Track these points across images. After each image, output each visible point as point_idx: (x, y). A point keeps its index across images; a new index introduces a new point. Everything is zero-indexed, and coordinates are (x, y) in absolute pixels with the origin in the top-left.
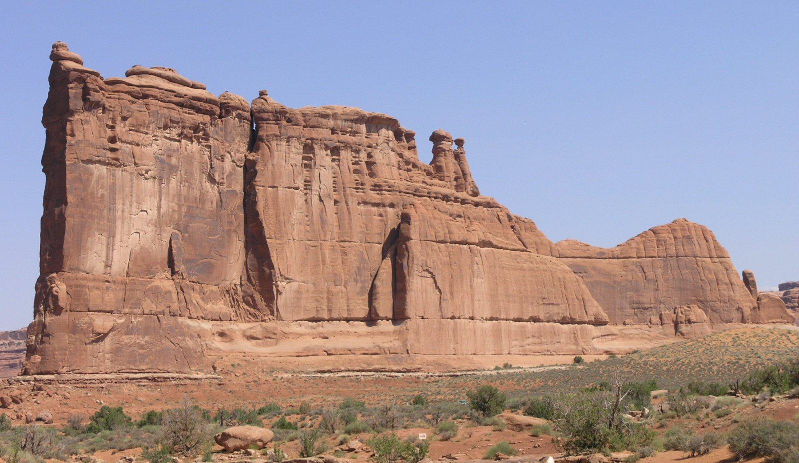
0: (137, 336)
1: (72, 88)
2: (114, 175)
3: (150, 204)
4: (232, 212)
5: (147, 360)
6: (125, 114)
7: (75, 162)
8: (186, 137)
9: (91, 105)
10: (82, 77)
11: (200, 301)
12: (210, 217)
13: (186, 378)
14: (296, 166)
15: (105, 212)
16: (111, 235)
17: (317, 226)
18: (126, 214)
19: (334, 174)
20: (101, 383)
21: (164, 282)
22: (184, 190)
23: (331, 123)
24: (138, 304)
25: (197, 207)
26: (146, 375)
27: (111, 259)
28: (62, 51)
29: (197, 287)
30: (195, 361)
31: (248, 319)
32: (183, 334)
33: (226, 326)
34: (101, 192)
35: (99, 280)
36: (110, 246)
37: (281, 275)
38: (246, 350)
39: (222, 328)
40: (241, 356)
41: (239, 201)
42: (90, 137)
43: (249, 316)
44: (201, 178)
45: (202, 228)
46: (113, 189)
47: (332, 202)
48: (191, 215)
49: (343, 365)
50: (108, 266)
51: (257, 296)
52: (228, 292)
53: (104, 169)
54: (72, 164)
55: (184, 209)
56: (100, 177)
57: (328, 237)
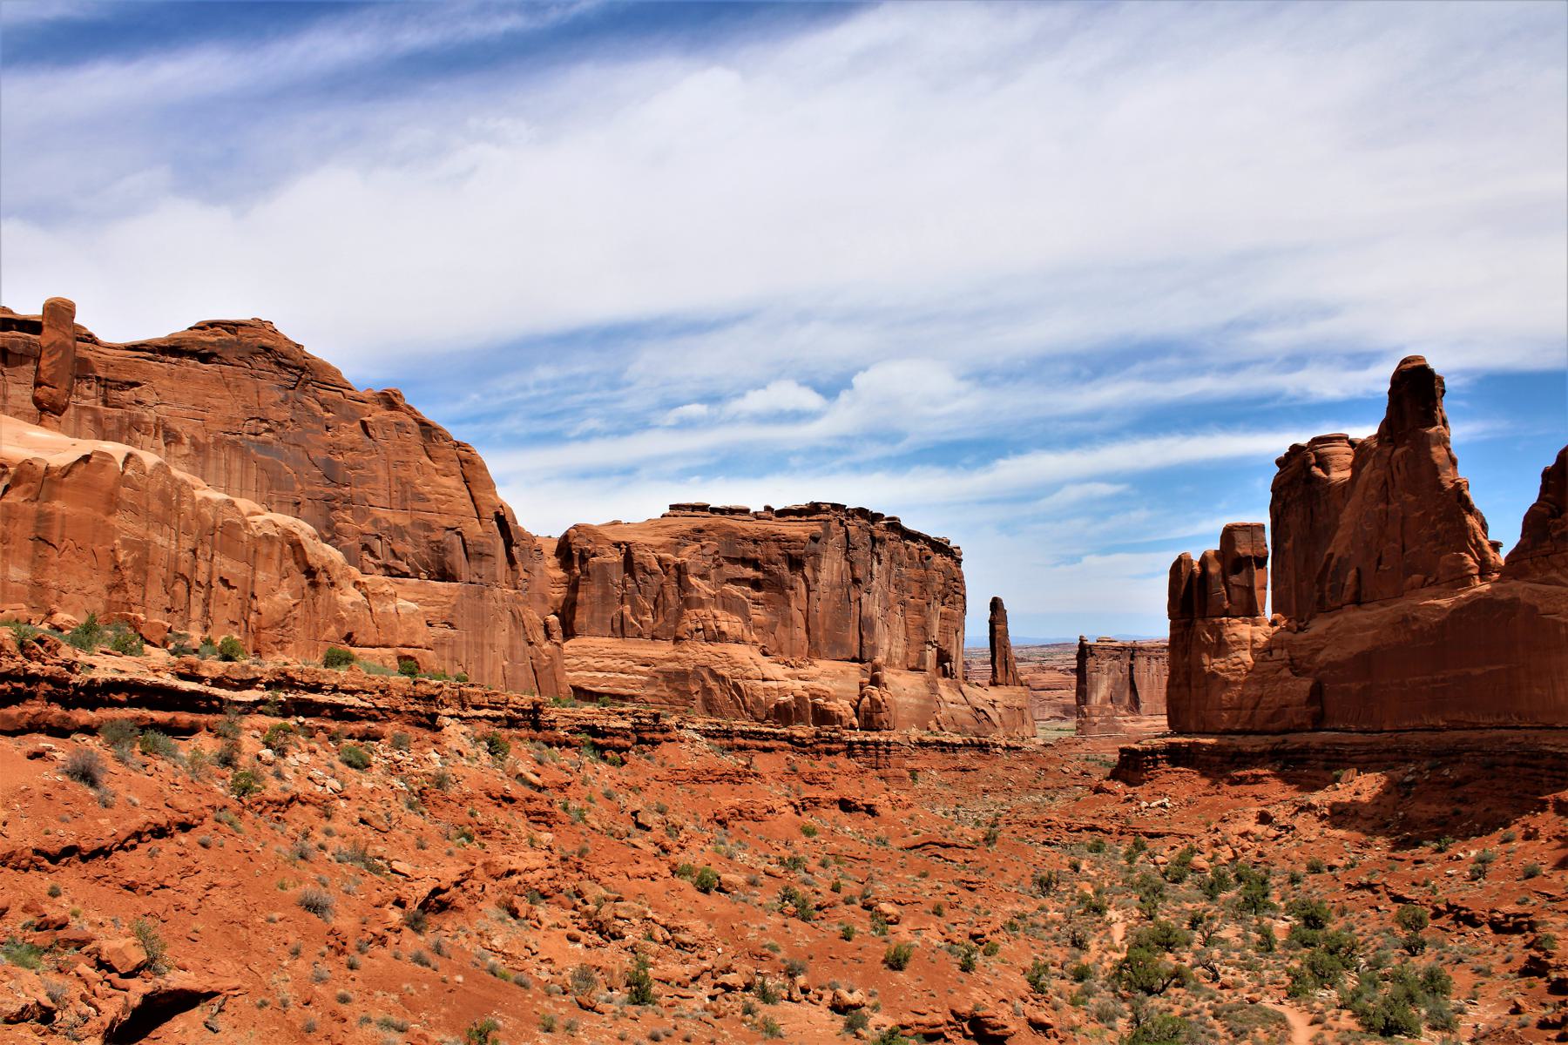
3: (1106, 682)
9: (1092, 655)
10: (1090, 647)
16: (1097, 692)
21: (1110, 706)
33: (1126, 718)
41: (1128, 677)
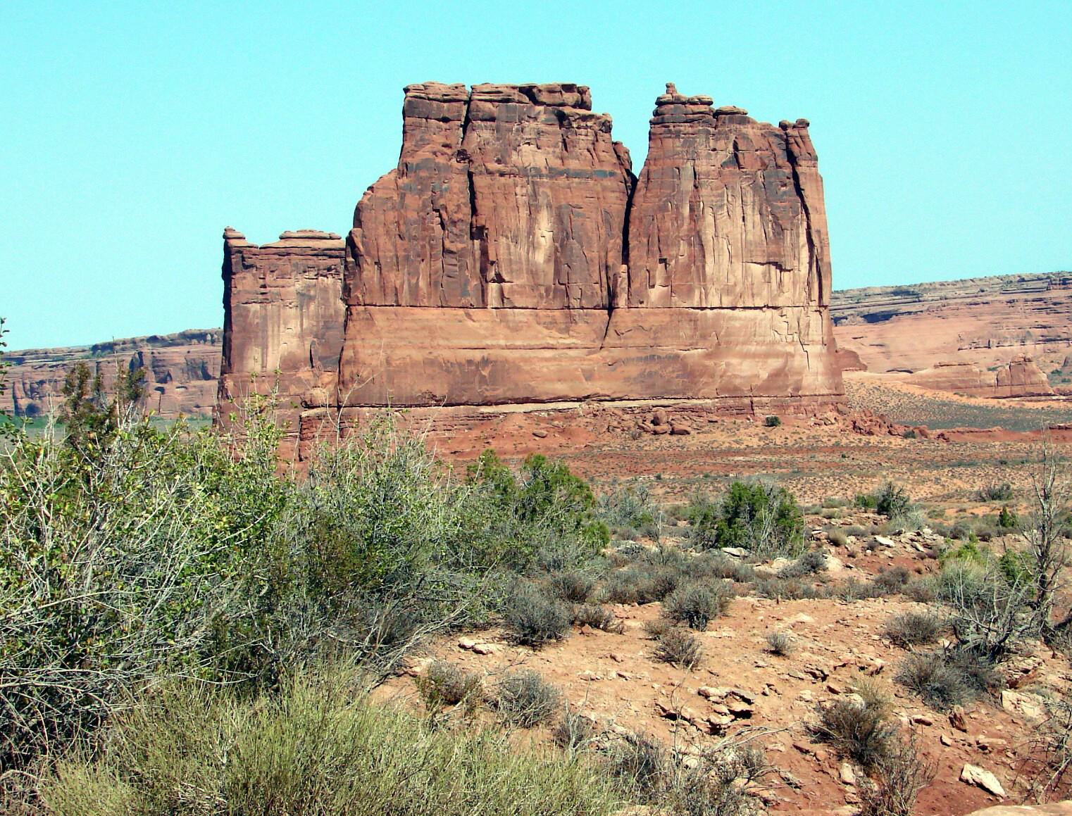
2: (266, 310)
6: (272, 269)
8: (321, 275)
9: (247, 267)
15: (260, 334)
16: (265, 347)
18: (276, 332)
21: (305, 373)
28: (230, 234)
34: (256, 321)
36: (264, 355)
42: (247, 288)
46: (265, 318)
48: (327, 327)
53: (258, 306)
55: (322, 324)
56: (256, 312)
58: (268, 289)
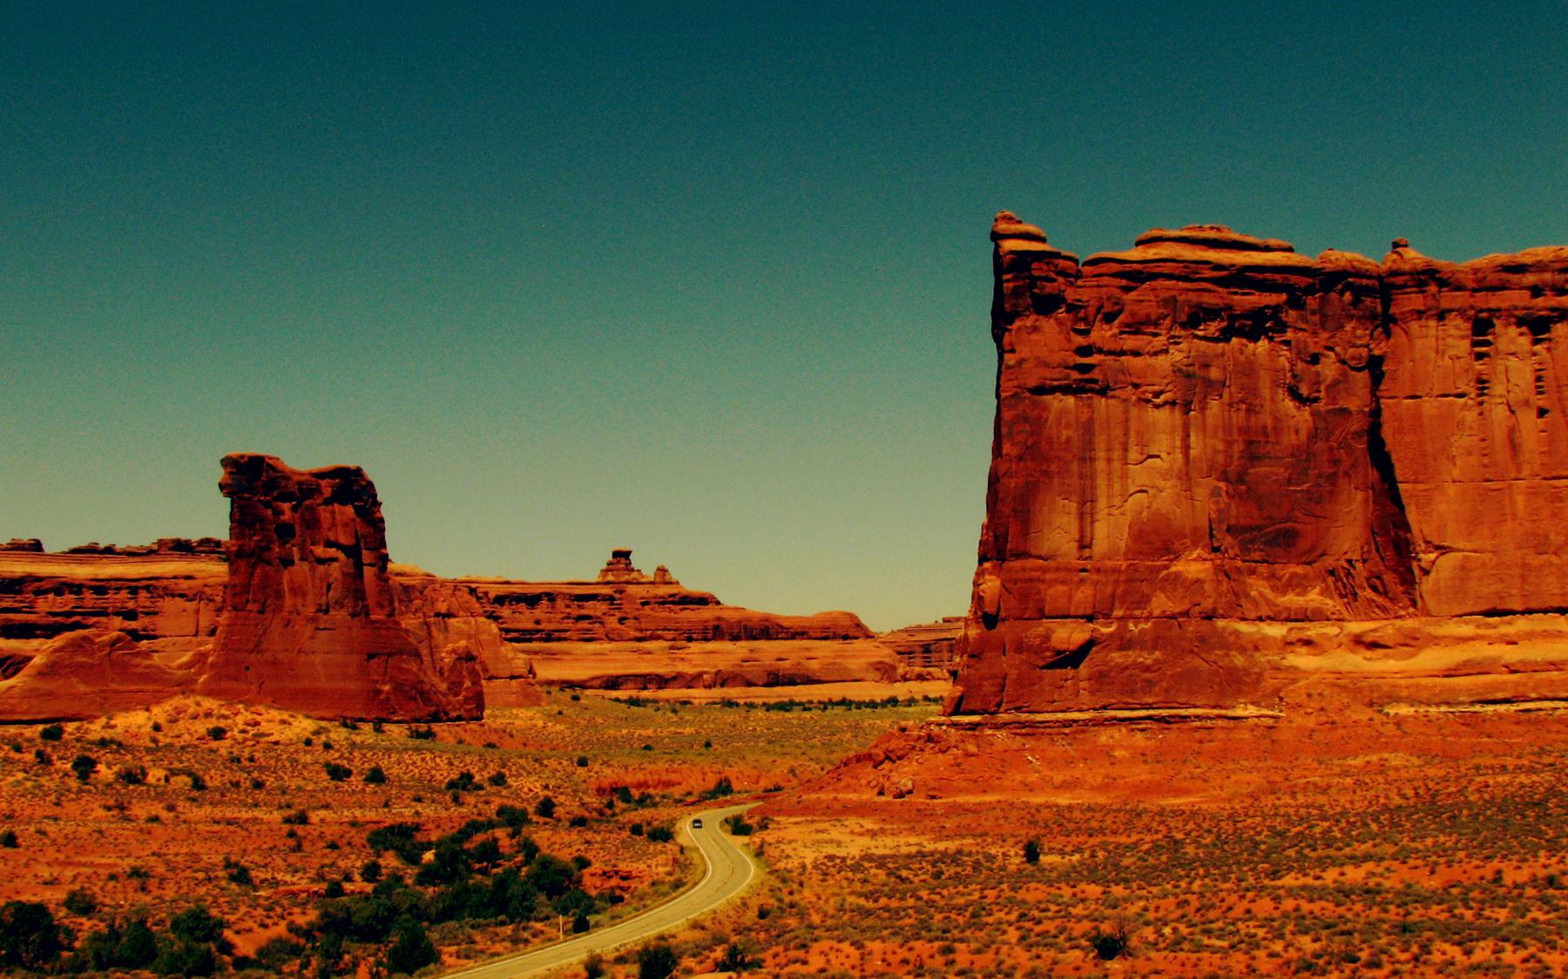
0: (1137, 652)
1: (1008, 281)
2: (1090, 406)
3: (1165, 444)
4: (1340, 444)
5: (1157, 688)
6: (1108, 308)
7: (1016, 393)
11: (1267, 592)
12: (1292, 455)
13: (1219, 717)
14: (1458, 358)
15: (1075, 467)
17: (1503, 454)
18: (1117, 465)
19: (1540, 364)
20: (1065, 726)
22: (1238, 418)
23: (1530, 279)
24: (1144, 601)
25: (1267, 442)
26: (1151, 712)
27: (1089, 535)
29: (1263, 569)
30: (1246, 688)
31: (1373, 615)
32: (1226, 647)
33: (1313, 630)
34: (1065, 434)
35: (1068, 569)
36: (1086, 515)
37: (1427, 542)
38: (1344, 668)
39: (1309, 633)
40: (1331, 678)
43: (1376, 610)
44: (1274, 394)
45: (1275, 474)
46: (1088, 429)
47: (1534, 413)
49: (1535, 689)
50: (1084, 544)
51: (1389, 578)
52: (1332, 573)
53: (1070, 400)
54: (1011, 396)
55: (1238, 448)
56: (1063, 412)
57: (1525, 473)
58: (1094, 359)
